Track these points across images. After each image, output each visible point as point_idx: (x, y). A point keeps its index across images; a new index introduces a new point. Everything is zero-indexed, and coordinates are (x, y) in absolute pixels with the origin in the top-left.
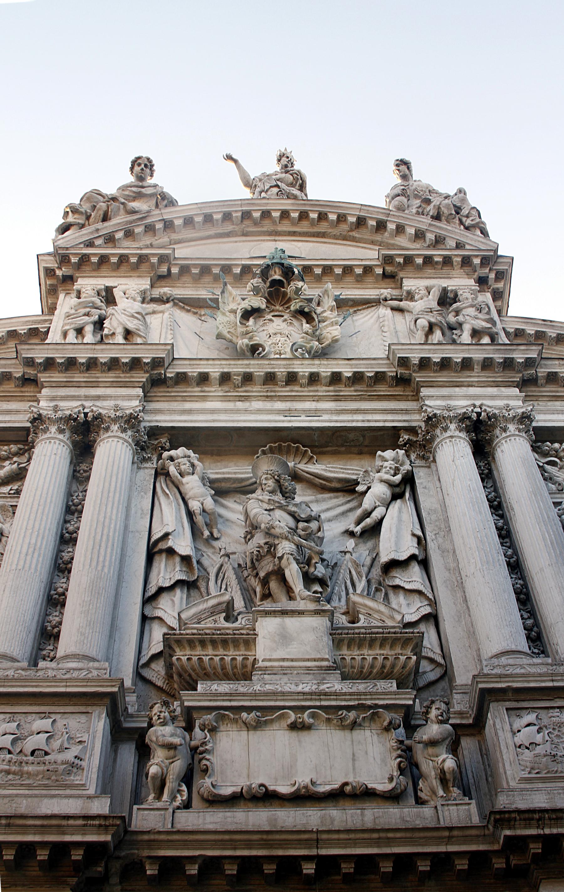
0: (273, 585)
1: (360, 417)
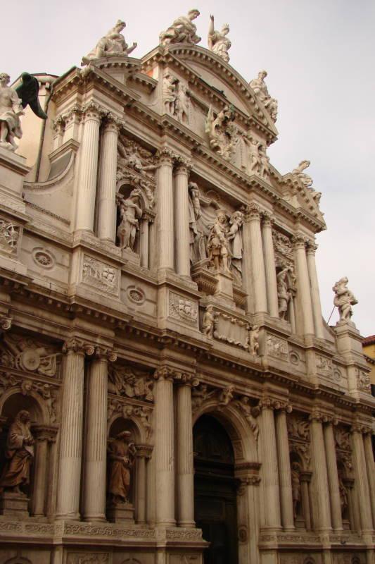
0: (217, 259)
1: (236, 194)
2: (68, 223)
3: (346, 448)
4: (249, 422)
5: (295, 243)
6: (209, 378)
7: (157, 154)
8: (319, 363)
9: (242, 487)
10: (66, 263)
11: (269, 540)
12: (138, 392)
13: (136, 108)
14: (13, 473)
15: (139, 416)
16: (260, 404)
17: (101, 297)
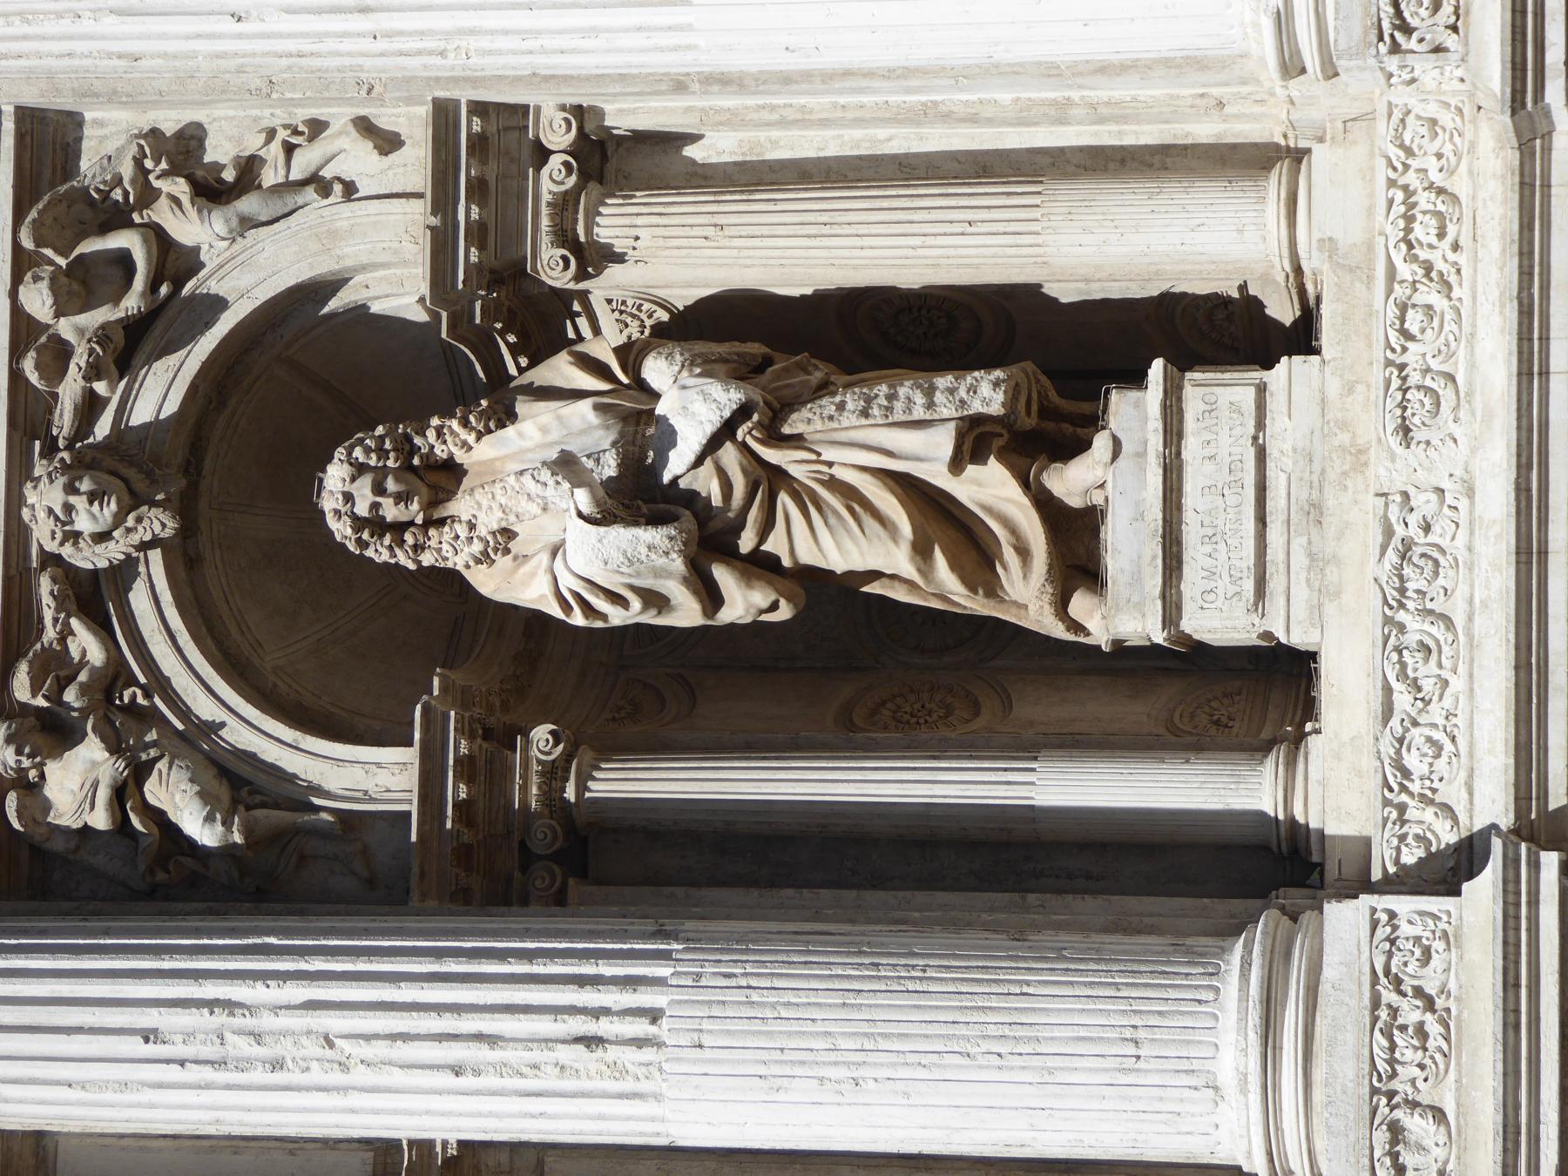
14: (922, 551)
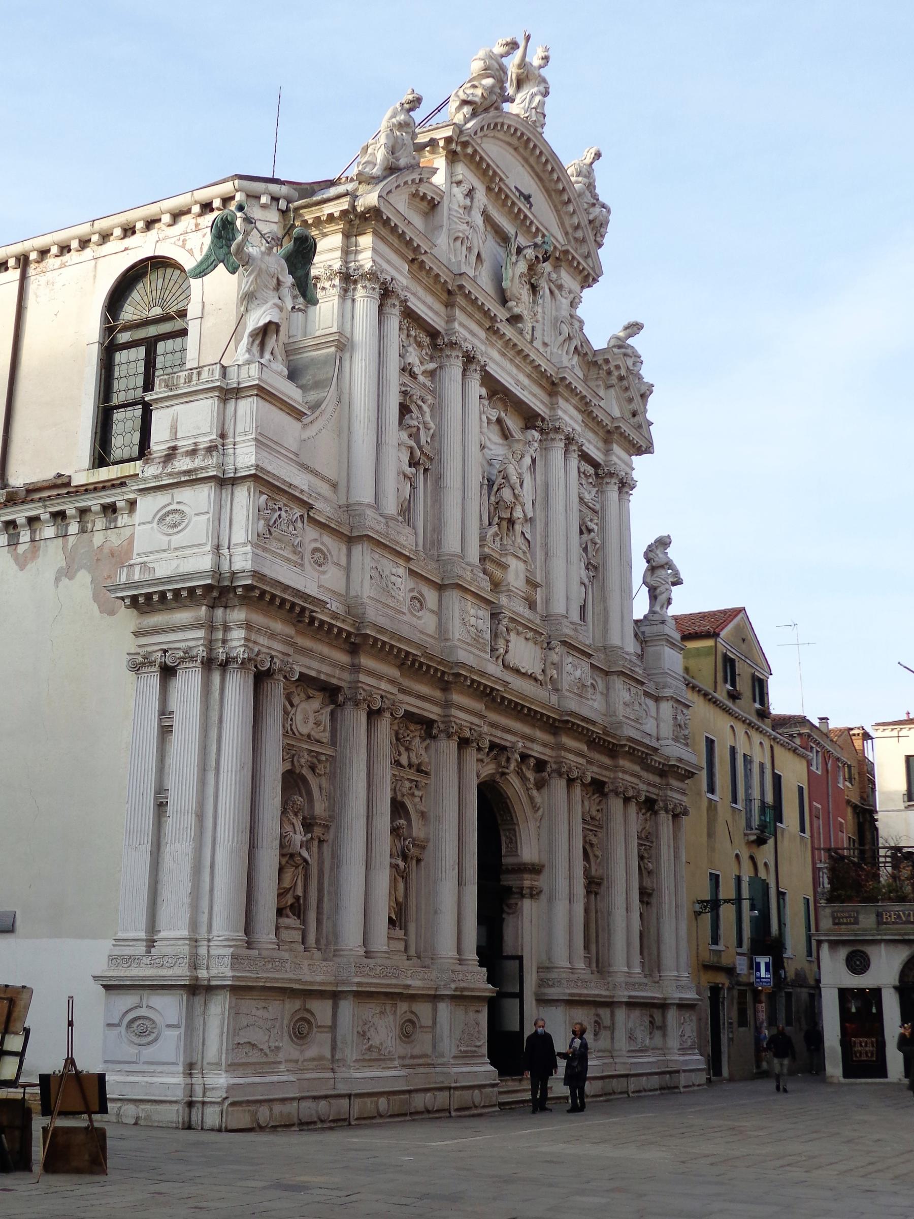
0: (504, 524)
2: (334, 486)
3: (647, 837)
4: (531, 798)
5: (603, 478)
6: (494, 732)
7: (439, 341)
8: (626, 696)
9: (513, 901)
10: (343, 561)
11: (552, 986)
12: (415, 761)
13: (423, 261)
14: (284, 888)
15: (413, 795)
16: (549, 770)
17: (392, 619)
